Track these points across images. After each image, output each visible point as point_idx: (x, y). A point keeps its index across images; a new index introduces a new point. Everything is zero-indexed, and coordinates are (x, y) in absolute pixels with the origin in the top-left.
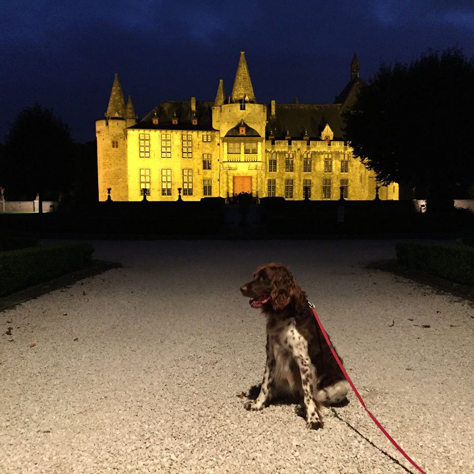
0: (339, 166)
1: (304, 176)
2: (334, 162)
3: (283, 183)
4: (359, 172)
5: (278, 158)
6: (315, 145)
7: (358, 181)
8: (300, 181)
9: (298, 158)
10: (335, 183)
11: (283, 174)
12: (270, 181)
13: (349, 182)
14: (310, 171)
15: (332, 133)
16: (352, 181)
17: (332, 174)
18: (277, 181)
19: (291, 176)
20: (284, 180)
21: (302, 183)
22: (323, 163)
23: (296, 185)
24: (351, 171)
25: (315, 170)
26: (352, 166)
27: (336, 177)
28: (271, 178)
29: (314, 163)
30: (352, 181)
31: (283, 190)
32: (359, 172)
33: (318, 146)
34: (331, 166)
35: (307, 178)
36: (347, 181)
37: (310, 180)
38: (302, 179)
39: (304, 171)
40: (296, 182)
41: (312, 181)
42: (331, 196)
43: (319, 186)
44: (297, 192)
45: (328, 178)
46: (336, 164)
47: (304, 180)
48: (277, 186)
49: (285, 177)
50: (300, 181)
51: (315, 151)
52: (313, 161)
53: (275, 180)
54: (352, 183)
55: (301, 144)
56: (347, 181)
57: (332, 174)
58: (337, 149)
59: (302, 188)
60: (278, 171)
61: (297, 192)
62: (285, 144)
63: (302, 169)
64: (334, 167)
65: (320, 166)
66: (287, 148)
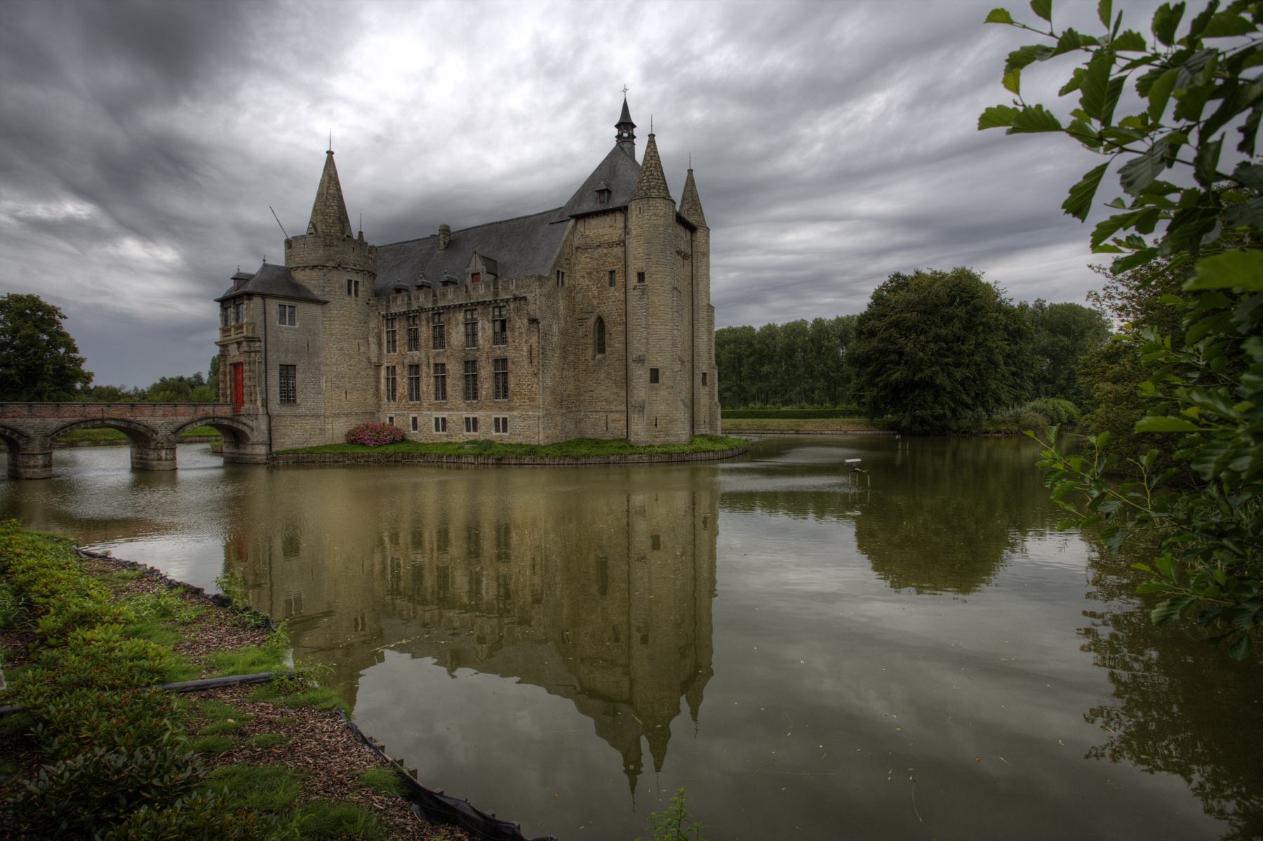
0: (490, 332)
1: (434, 358)
2: (480, 325)
3: (406, 373)
4: (527, 342)
5: (397, 327)
6: (444, 295)
7: (526, 362)
8: (428, 366)
9: (424, 323)
10: (484, 368)
11: (403, 356)
12: (388, 368)
13: (510, 364)
14: (443, 347)
15: (484, 267)
16: (513, 363)
17: (478, 350)
18: (397, 368)
19: (416, 358)
20: (407, 368)
21: (432, 371)
22: (462, 328)
23: (424, 375)
24: (510, 340)
25: (449, 343)
26: (513, 330)
27: (485, 355)
28: (389, 365)
29: (448, 331)
30: (513, 363)
31: (406, 387)
32: (527, 342)
33: (450, 296)
34: (475, 334)
35: (439, 361)
36: (505, 360)
37: (443, 365)
38: (432, 362)
39: (435, 348)
40: (424, 368)
41: (447, 367)
42: (479, 395)
43: (458, 376)
44: (425, 389)
45: (471, 359)
46: (483, 328)
47: (436, 365)
48: (398, 379)
49: (406, 361)
50: (428, 366)
51: (445, 307)
52: (446, 327)
53: (394, 367)
54: (514, 367)
55: (425, 295)
56: (505, 360)
57: (478, 350)
58: (483, 296)
59: (432, 379)
60: (398, 351)
61: (425, 389)
62: (403, 300)
63: (431, 344)
64: (480, 334)
65: (456, 335)
66: (406, 306)
